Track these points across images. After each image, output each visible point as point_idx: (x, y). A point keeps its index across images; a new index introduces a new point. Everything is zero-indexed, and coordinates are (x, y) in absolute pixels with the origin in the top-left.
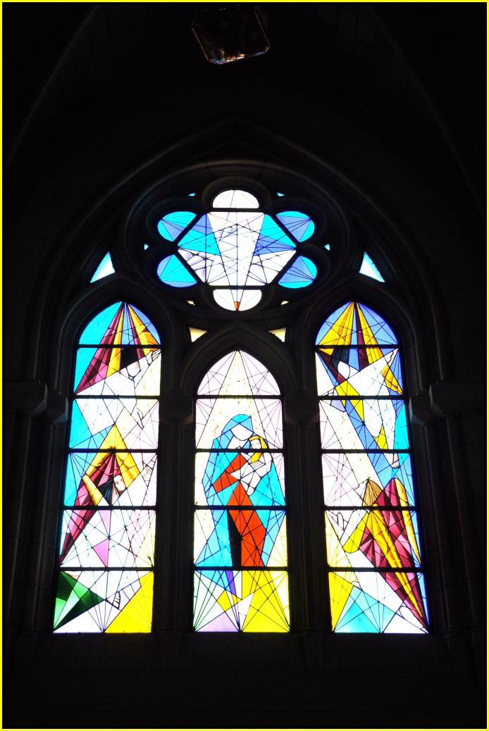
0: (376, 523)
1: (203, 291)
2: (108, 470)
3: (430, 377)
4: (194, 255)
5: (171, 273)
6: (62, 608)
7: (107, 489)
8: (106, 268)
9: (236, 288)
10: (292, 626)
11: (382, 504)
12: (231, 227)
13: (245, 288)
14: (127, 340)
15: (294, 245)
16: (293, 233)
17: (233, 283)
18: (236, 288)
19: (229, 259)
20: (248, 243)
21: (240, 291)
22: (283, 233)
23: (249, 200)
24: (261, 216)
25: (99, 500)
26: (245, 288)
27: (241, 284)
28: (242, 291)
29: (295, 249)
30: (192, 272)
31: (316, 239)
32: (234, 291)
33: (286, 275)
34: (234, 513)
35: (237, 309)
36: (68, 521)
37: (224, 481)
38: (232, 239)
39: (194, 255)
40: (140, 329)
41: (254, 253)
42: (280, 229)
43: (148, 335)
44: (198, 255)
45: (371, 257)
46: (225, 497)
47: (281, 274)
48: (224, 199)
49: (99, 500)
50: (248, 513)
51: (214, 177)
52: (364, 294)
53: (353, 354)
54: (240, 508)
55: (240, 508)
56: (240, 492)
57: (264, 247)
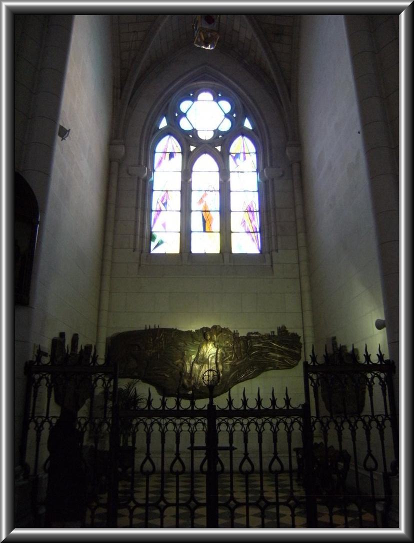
0: (246, 216)
1: (194, 132)
2: (165, 198)
3: (265, 166)
5: (184, 125)
6: (153, 244)
7: (165, 204)
8: (163, 123)
10: (220, 251)
11: (248, 210)
14: (171, 151)
25: (163, 208)
31: (231, 113)
34: (204, 213)
36: (154, 214)
37: (201, 201)
40: (175, 146)
43: (178, 149)
45: (248, 119)
46: (201, 208)
49: (163, 208)
50: (208, 213)
51: (199, 88)
52: (244, 133)
53: (242, 155)
54: (206, 211)
55: (206, 211)
56: (205, 206)
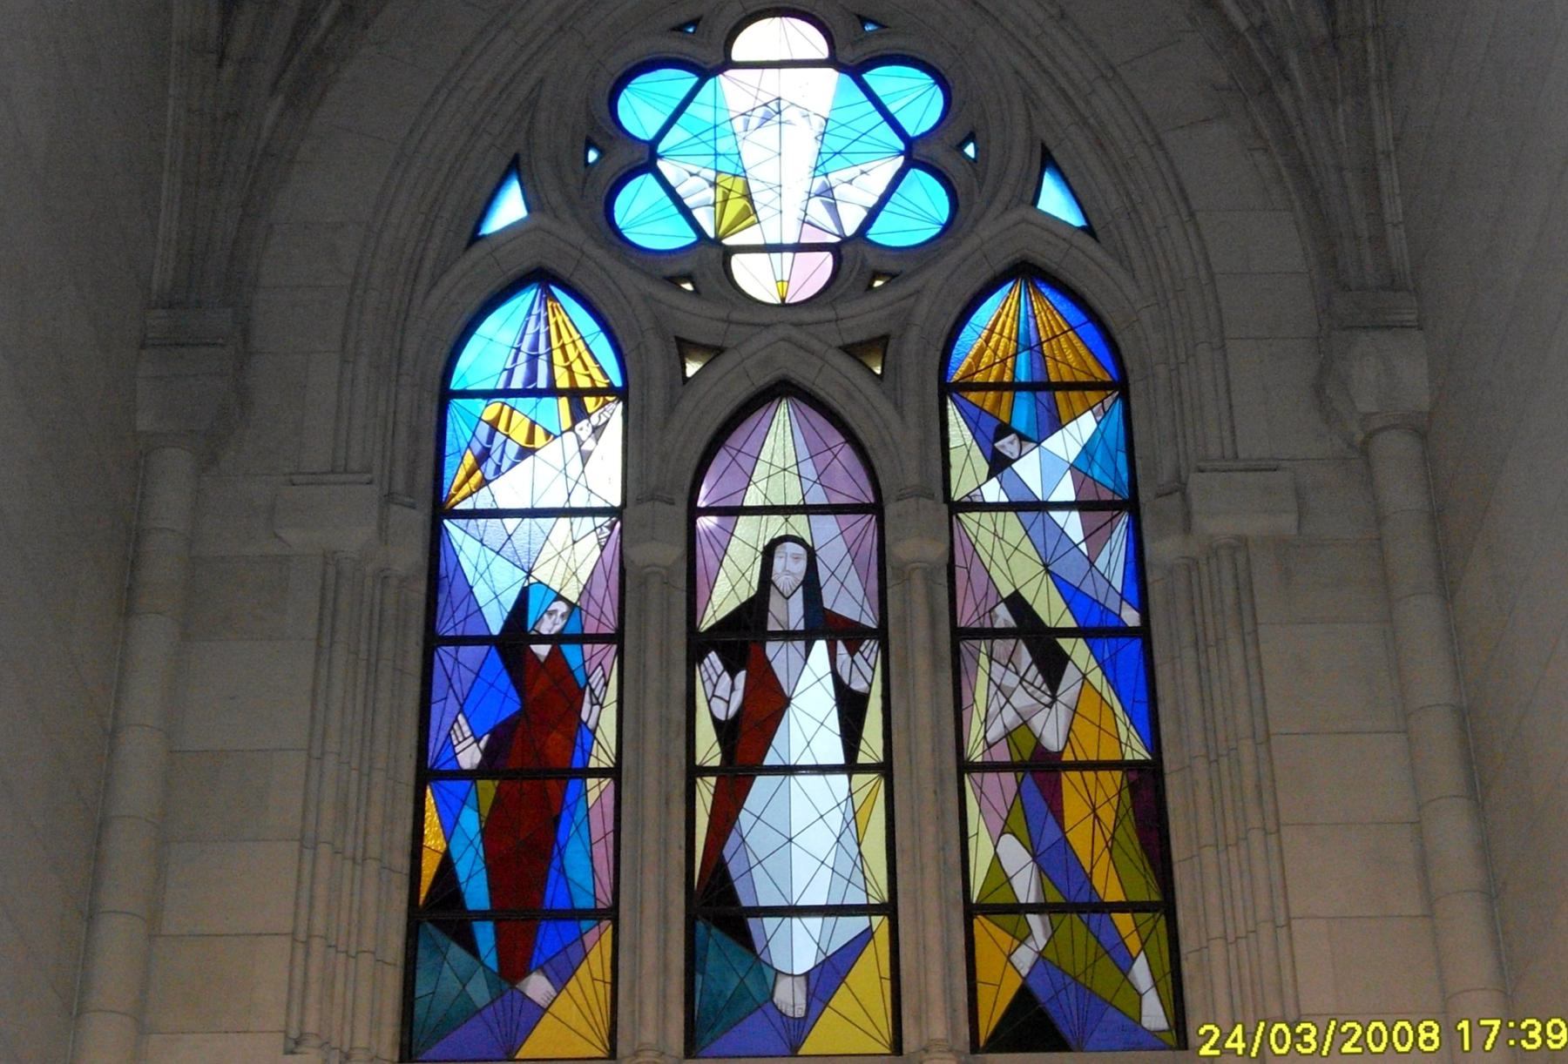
4: (692, 175)
8: (510, 208)
9: (779, 248)
12: (766, 105)
13: (799, 248)
15: (901, 146)
16: (900, 118)
17: (773, 239)
18: (779, 248)
19: (763, 186)
20: (801, 144)
21: (788, 256)
22: (878, 117)
23: (806, 40)
24: (830, 77)
26: (799, 248)
27: (791, 239)
28: (790, 255)
29: (901, 153)
30: (686, 212)
32: (776, 256)
33: (882, 214)
35: (783, 299)
38: (771, 129)
39: (692, 175)
41: (816, 169)
42: (870, 106)
44: (697, 175)
47: (873, 214)
48: (758, 40)
57: (835, 154)
